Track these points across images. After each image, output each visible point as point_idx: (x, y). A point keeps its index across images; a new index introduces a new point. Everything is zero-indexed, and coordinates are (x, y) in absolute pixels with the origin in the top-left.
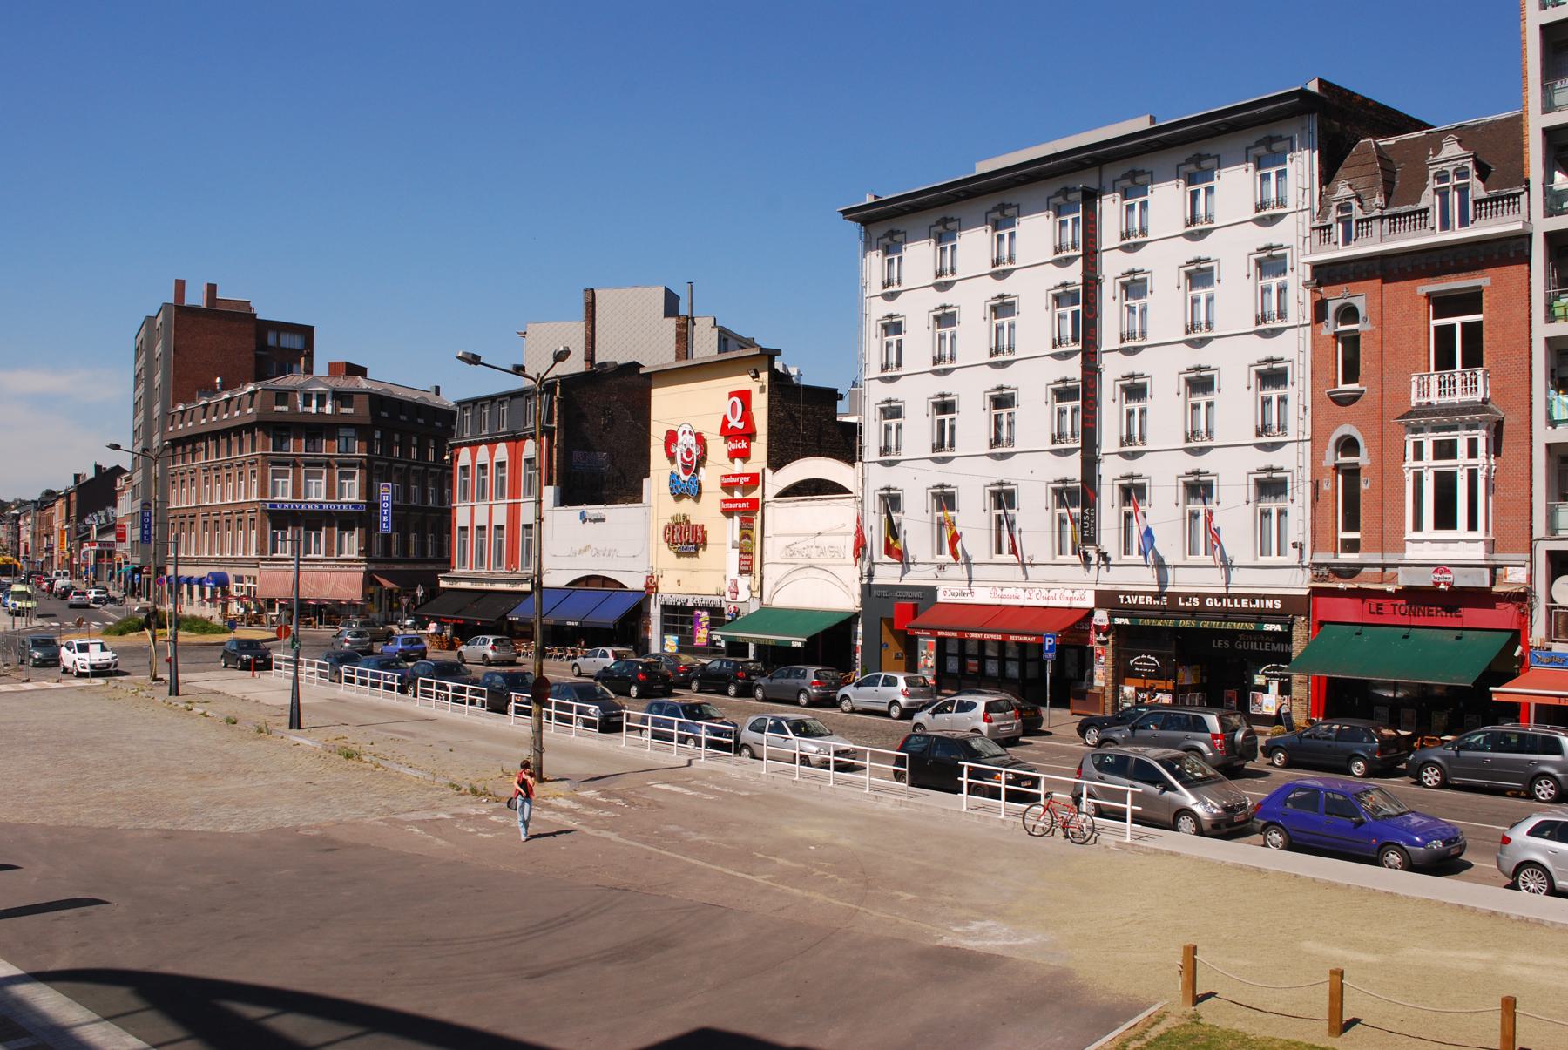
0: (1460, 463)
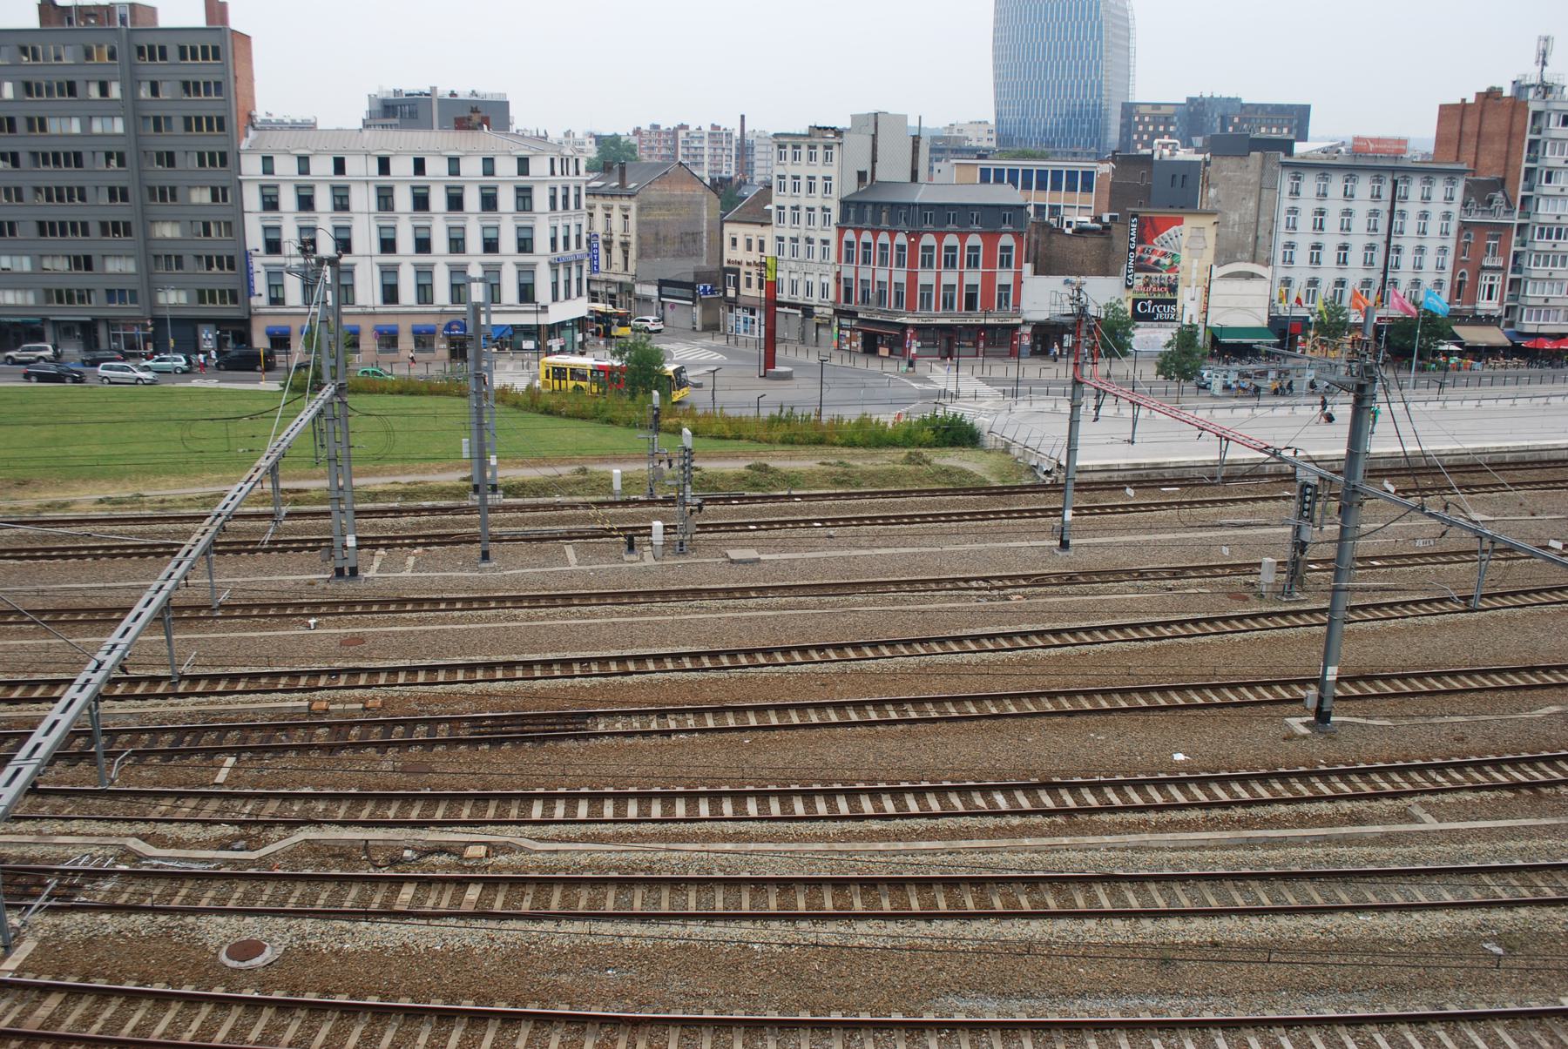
0: (1495, 282)
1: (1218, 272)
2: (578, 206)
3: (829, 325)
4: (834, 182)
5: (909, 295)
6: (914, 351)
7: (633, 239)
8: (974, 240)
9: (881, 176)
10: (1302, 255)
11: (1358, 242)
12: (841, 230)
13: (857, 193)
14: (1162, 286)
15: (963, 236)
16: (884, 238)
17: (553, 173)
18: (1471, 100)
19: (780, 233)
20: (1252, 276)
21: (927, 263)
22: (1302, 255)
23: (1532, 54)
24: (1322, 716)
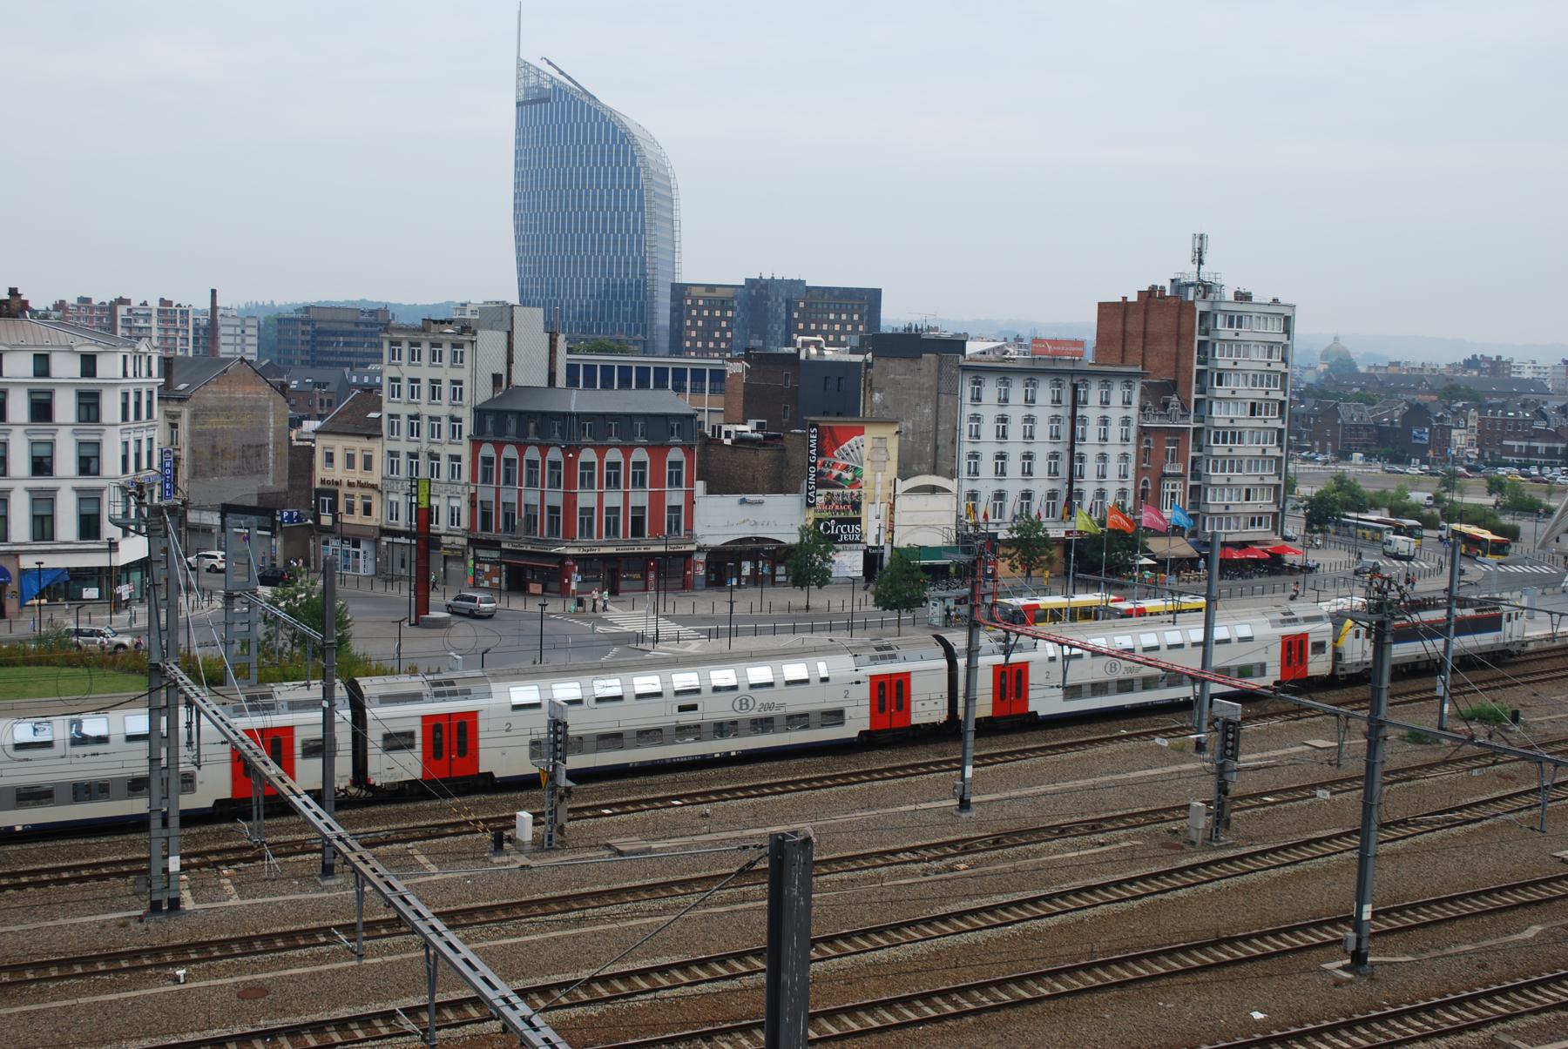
1: (902, 486)
2: (150, 415)
3: (461, 558)
4: (466, 387)
5: (562, 519)
6: (573, 586)
7: (184, 454)
8: (640, 455)
9: (517, 380)
10: (987, 466)
11: (1042, 450)
12: (476, 444)
13: (492, 400)
14: (845, 503)
15: (627, 450)
16: (532, 453)
17: (125, 375)
18: (1133, 298)
19: (393, 446)
20: (934, 490)
21: (587, 482)
22: (987, 466)
23: (1189, 254)
24: (1358, 958)
